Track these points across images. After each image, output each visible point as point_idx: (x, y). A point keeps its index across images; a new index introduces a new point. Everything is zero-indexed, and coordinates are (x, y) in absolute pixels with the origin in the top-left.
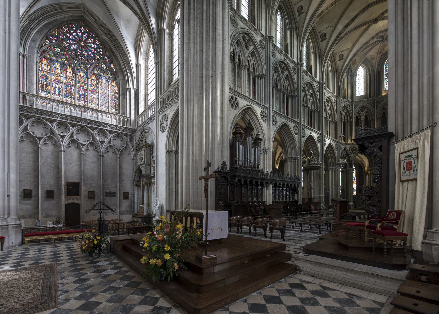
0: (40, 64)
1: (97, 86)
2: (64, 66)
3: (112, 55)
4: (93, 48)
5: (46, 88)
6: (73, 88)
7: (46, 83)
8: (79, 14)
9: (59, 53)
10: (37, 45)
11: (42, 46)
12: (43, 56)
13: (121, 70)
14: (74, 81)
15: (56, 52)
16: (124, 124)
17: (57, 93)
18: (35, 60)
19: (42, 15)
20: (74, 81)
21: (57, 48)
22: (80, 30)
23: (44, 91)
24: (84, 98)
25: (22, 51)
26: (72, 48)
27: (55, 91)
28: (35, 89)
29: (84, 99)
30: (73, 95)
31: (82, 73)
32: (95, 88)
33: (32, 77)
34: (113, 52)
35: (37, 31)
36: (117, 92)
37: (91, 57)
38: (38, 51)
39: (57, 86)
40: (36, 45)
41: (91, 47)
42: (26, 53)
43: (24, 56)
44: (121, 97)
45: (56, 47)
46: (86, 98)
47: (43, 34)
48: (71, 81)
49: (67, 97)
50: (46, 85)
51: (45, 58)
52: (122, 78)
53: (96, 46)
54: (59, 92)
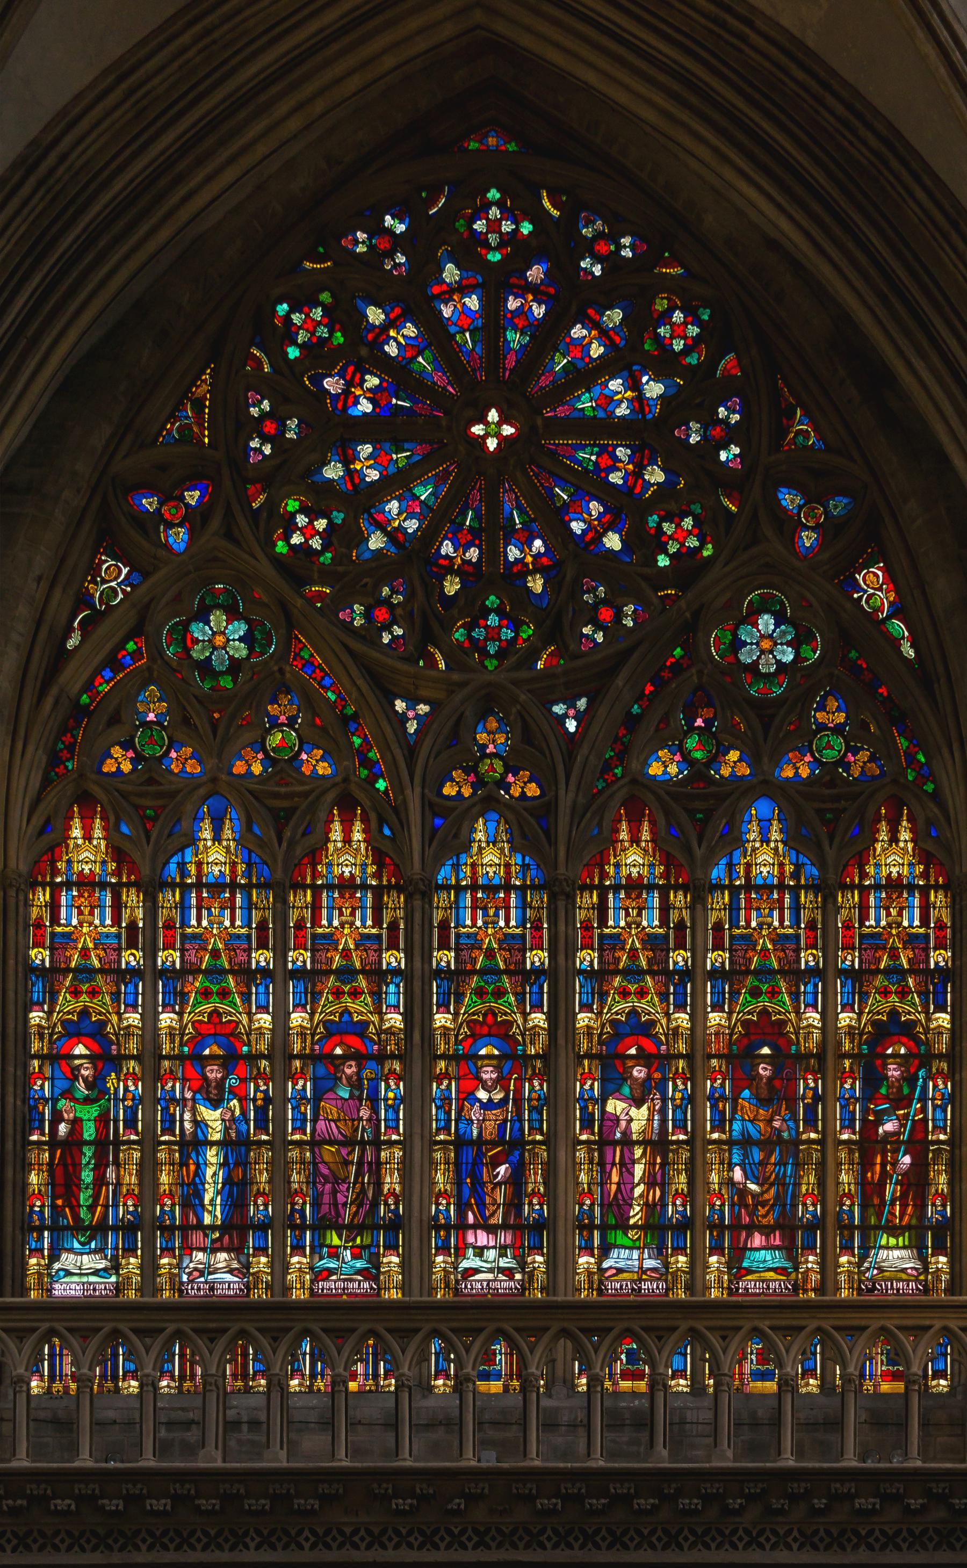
1: (679, 958)
5: (100, 1181)
6: (390, 1091)
7: (102, 1120)
14: (393, 993)
20: (393, 993)
23: (78, 1227)
24: (517, 1180)
27: (192, 1196)
30: (391, 1181)
31: (490, 857)
46: (535, 1180)
48: (360, 1008)
50: (101, 1144)
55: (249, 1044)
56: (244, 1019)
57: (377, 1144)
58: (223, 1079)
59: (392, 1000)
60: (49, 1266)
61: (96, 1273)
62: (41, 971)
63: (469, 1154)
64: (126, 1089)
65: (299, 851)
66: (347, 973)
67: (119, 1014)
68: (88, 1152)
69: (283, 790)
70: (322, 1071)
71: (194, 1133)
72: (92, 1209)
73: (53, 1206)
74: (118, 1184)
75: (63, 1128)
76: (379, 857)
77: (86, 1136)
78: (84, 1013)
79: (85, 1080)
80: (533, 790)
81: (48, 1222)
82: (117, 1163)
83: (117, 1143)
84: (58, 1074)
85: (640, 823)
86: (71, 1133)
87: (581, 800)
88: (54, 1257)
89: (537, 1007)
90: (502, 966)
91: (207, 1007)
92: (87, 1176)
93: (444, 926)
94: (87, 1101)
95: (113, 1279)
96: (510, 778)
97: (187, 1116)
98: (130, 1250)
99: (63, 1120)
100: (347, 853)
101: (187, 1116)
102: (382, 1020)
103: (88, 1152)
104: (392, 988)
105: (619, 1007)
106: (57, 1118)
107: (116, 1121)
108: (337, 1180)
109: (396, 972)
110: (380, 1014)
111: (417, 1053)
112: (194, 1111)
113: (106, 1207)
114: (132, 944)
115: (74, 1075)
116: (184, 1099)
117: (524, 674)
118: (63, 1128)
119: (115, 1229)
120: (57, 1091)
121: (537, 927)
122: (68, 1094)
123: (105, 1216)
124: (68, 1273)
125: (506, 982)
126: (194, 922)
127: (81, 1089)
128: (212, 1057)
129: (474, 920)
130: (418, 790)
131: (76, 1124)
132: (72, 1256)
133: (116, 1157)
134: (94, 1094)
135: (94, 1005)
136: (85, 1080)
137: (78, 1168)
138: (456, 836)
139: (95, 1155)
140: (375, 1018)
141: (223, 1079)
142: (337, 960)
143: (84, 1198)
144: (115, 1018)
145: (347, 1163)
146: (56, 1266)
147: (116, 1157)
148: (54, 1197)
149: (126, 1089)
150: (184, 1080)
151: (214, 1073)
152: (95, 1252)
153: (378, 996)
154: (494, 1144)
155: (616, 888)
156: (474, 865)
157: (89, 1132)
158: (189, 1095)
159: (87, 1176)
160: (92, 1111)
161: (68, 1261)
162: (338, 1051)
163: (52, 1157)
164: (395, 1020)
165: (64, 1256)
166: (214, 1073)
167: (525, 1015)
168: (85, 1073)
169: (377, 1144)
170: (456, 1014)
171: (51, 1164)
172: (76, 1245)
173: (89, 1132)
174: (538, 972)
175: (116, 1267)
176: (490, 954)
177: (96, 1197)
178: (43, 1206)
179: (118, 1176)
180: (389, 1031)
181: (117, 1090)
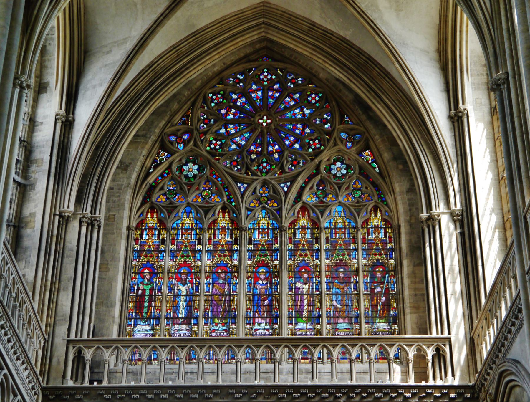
0: (139, 232)
1: (316, 246)
2: (206, 213)
3: (363, 117)
4: (300, 121)
5: (150, 306)
7: (151, 290)
8: (254, 36)
9: (195, 176)
10: (134, 176)
11: (148, 174)
12: (147, 206)
13: (400, 158)
15: (186, 177)
16: (422, 375)
17: (182, 313)
18: (125, 224)
19: (151, 83)
20: (235, 256)
21: (190, 165)
22: (259, 82)
23: (142, 318)
25: (88, 211)
26: (234, 146)
27: (176, 310)
28: (117, 320)
29: (269, 311)
30: (234, 305)
32: (308, 259)
33: (112, 281)
34: (367, 109)
35: (136, 136)
36: (390, 246)
37: (294, 152)
38: (135, 192)
39: (183, 289)
40: (129, 177)
41: (294, 120)
42: (101, 215)
43: (92, 224)
44: (405, 262)
45: (186, 164)
47: (153, 138)
48: (226, 260)
49: (213, 318)
50: (151, 296)
51: (152, 209)
52: (406, 185)
53: (307, 111)
54: (190, 307)
55: (194, 269)
56: (193, 263)
57: (230, 295)
58: (187, 278)
59: (235, 257)
60: (133, 329)
61: (147, 331)
62: (137, 251)
63: (256, 298)
64: (159, 281)
65: (210, 221)
66: (223, 251)
67: (158, 262)
68: (147, 298)
69: (206, 205)
70: (215, 276)
71: (177, 293)
72: (147, 313)
73: (136, 313)
74: (155, 306)
75: (140, 292)
76: (232, 221)
77: (146, 294)
78: (148, 262)
79: (147, 279)
80: (275, 205)
81: (134, 317)
82: (155, 301)
83: (155, 296)
84: (140, 277)
85: (305, 212)
86: (142, 293)
87: (289, 207)
88: (135, 326)
89: (277, 259)
90: (266, 248)
91: (183, 260)
92: (146, 304)
93: (250, 239)
94: (147, 284)
95: (152, 332)
96: (269, 202)
97: (176, 288)
98: (157, 325)
99: (140, 289)
100: (224, 221)
101: (176, 288)
102: (232, 263)
103: (147, 298)
104: (235, 254)
105: (299, 259)
106: (139, 289)
107: (155, 290)
108: (218, 305)
109: (237, 250)
110: (232, 261)
111: (242, 271)
112: (178, 287)
113: (151, 313)
114: (163, 243)
115: (144, 278)
116: (175, 284)
117: (273, 177)
118: (140, 292)
119: (153, 318)
120: (139, 282)
121: (276, 239)
122: (142, 283)
123: (150, 315)
124: (139, 331)
125: (267, 252)
126: (180, 238)
127: (146, 281)
128: (184, 273)
129: (259, 237)
130: (244, 205)
131: (144, 290)
132: (140, 326)
133: (155, 299)
134: (149, 283)
135: (151, 259)
136: (147, 279)
137: (144, 302)
138: (254, 216)
139: (149, 299)
140: (230, 262)
141: (187, 278)
142: (220, 248)
143: (145, 310)
144: (157, 263)
145: (221, 301)
146: (135, 329)
147: (155, 299)
148: (136, 310)
149: (159, 281)
150: (175, 279)
151: (184, 277)
152: (147, 325)
153: (231, 256)
154: (264, 295)
155: (299, 229)
156: (259, 223)
157: (147, 292)
158: (176, 283)
159: (146, 304)
160: (149, 287)
161: (139, 327)
162: (220, 271)
163: (136, 299)
164: (236, 263)
165: (138, 326)
166: (184, 277)
167: (273, 261)
168: (147, 277)
169: (230, 295)
170: (253, 261)
171: (136, 301)
172: (142, 323)
173: (147, 292)
174: (277, 250)
175: (153, 329)
176: (263, 245)
177: (148, 310)
178: (132, 313)
179: (155, 304)
180: (235, 266)
181: (156, 281)
